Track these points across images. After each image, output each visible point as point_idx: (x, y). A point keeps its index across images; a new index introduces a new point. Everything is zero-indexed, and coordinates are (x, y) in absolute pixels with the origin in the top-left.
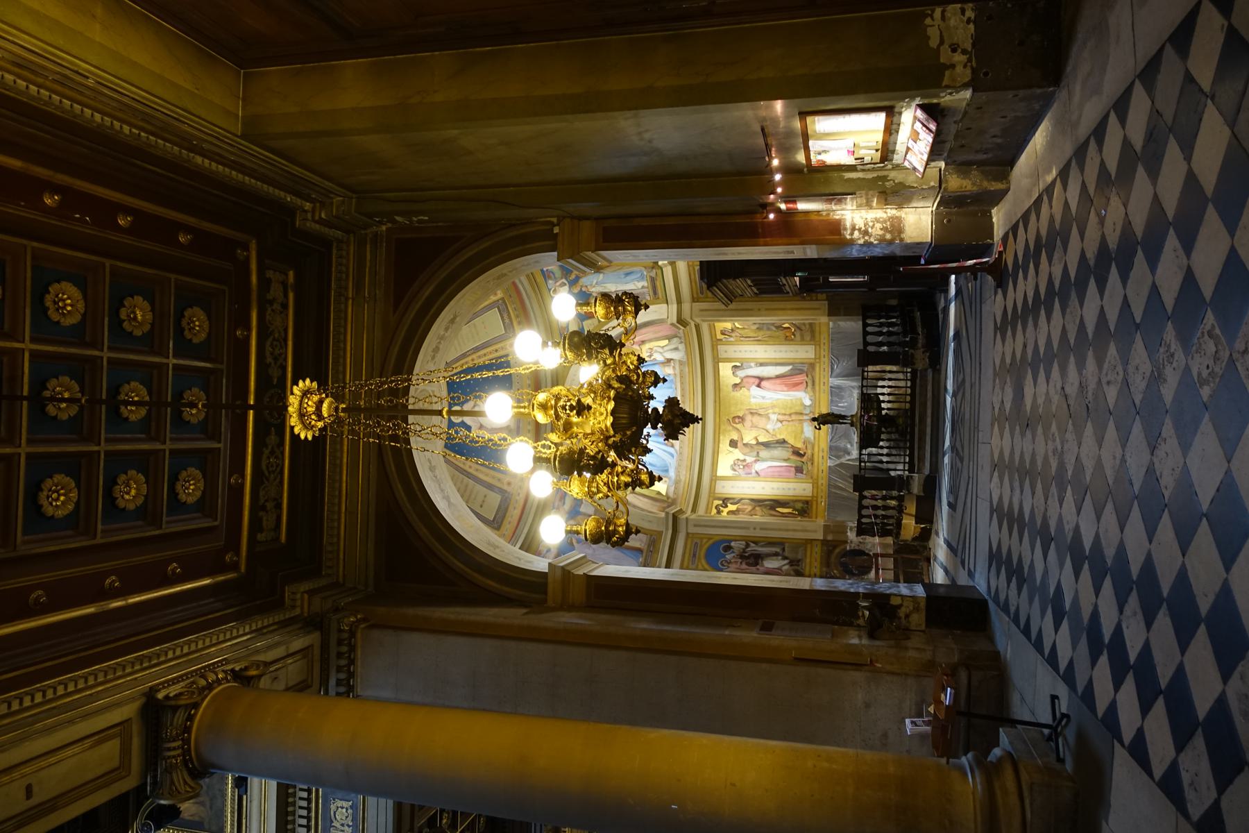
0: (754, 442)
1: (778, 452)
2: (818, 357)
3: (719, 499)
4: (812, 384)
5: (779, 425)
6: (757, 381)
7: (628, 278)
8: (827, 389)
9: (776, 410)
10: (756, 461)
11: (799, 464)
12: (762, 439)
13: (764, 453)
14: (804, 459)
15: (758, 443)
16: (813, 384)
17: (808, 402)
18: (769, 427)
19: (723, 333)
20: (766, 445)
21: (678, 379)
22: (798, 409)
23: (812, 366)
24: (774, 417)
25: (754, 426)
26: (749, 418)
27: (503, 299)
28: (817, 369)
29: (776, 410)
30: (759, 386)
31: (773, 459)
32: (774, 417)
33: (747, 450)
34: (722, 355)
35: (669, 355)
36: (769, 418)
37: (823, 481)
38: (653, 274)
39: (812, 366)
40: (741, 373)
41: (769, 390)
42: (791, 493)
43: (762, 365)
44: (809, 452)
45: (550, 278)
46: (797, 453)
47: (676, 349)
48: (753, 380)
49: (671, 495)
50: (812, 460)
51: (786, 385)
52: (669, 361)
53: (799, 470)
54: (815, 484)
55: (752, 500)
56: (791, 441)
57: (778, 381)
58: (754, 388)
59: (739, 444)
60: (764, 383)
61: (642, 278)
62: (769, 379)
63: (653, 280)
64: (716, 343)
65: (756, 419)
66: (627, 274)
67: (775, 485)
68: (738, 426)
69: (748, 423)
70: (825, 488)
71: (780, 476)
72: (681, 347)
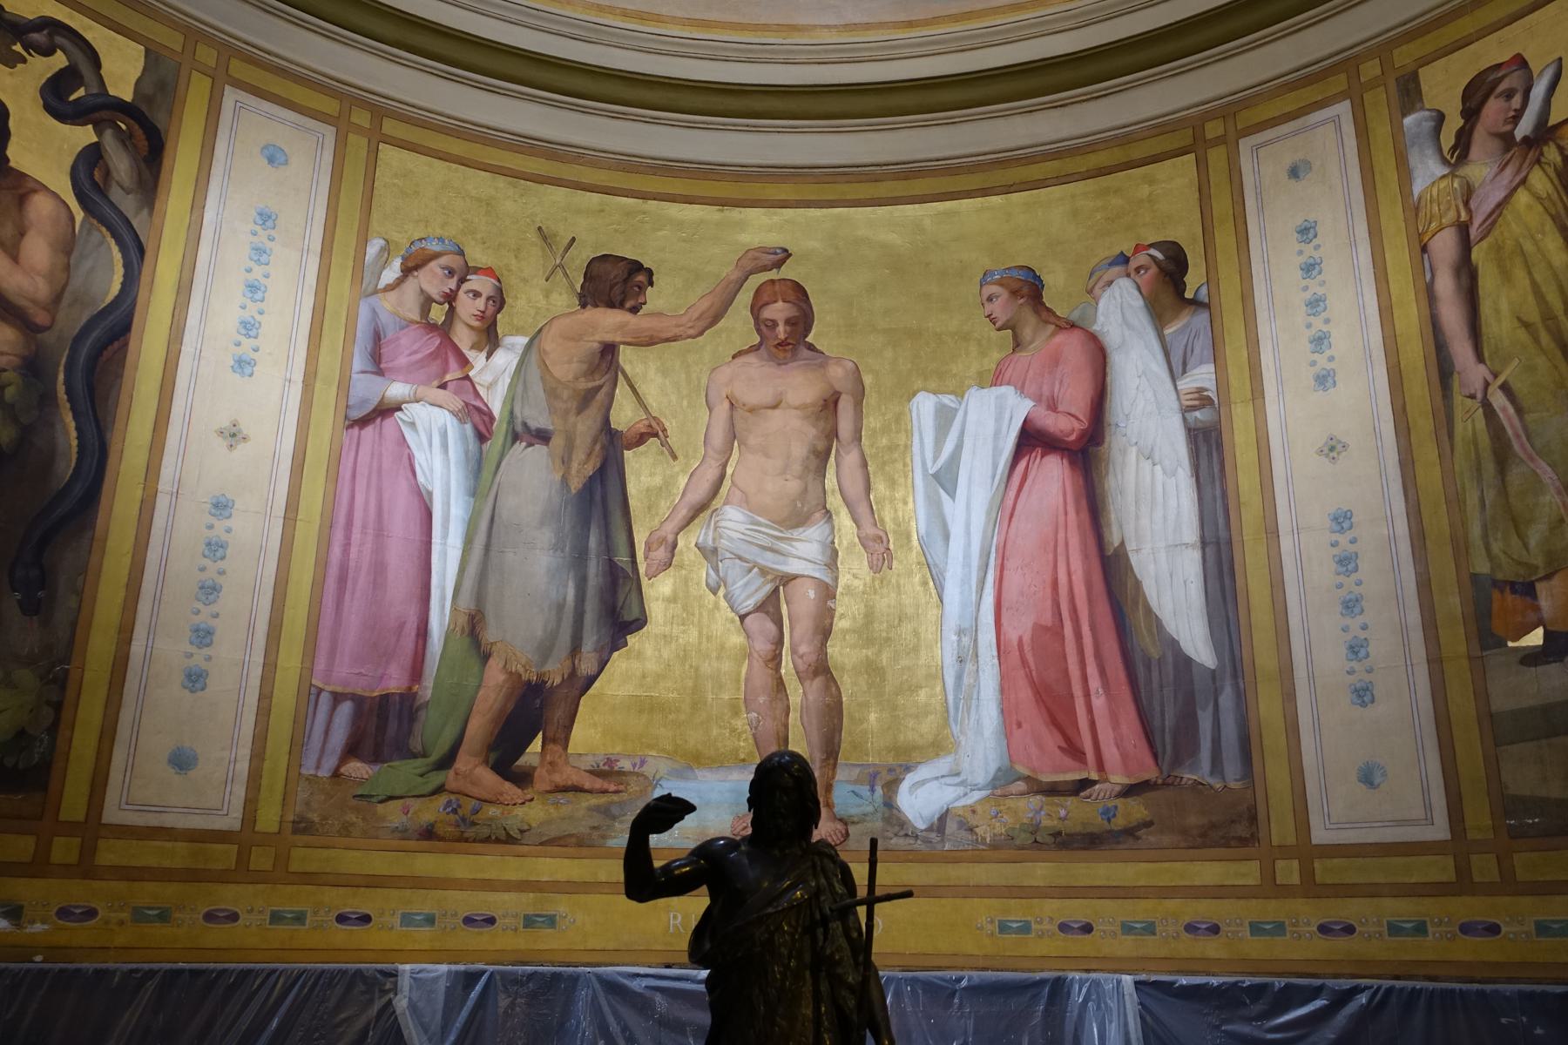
0: (624, 415)
1: (538, 574)
2: (1319, 872)
3: (162, 81)
4: (1061, 821)
5: (750, 592)
6: (1065, 425)
8: (1040, 949)
9: (854, 571)
10: (479, 421)
11: (434, 731)
12: (642, 472)
13: (533, 479)
14: (474, 771)
15: (612, 448)
16: (1067, 842)
17: (921, 799)
18: (733, 520)
19: (1475, 96)
20: (599, 499)
22: (868, 723)
23: (1234, 826)
24: (802, 553)
25: (738, 421)
26: (800, 386)
28: (1208, 872)
29: (854, 571)
30: (1031, 440)
31: (488, 537)
32: (802, 553)
33: (567, 365)
34: (1262, 162)
36: (796, 519)
37: (255, 928)
39: (1234, 826)
40: (1120, 312)
41: (1006, 511)
42: (161, 646)
43: (1207, 443)
44: (533, 812)
46: (534, 712)
48: (1076, 397)
50: (467, 831)
51: (1049, 634)
53: (382, 726)
54: (236, 855)
55: (113, 330)
56: (628, 673)
57: (1077, 567)
58: (1016, 407)
59: (608, 322)
60: (1052, 474)
62: (1093, 505)
65: (790, 432)
67: (255, 530)
68: (739, 325)
69: (757, 380)
70: (187, 936)
71: (335, 580)
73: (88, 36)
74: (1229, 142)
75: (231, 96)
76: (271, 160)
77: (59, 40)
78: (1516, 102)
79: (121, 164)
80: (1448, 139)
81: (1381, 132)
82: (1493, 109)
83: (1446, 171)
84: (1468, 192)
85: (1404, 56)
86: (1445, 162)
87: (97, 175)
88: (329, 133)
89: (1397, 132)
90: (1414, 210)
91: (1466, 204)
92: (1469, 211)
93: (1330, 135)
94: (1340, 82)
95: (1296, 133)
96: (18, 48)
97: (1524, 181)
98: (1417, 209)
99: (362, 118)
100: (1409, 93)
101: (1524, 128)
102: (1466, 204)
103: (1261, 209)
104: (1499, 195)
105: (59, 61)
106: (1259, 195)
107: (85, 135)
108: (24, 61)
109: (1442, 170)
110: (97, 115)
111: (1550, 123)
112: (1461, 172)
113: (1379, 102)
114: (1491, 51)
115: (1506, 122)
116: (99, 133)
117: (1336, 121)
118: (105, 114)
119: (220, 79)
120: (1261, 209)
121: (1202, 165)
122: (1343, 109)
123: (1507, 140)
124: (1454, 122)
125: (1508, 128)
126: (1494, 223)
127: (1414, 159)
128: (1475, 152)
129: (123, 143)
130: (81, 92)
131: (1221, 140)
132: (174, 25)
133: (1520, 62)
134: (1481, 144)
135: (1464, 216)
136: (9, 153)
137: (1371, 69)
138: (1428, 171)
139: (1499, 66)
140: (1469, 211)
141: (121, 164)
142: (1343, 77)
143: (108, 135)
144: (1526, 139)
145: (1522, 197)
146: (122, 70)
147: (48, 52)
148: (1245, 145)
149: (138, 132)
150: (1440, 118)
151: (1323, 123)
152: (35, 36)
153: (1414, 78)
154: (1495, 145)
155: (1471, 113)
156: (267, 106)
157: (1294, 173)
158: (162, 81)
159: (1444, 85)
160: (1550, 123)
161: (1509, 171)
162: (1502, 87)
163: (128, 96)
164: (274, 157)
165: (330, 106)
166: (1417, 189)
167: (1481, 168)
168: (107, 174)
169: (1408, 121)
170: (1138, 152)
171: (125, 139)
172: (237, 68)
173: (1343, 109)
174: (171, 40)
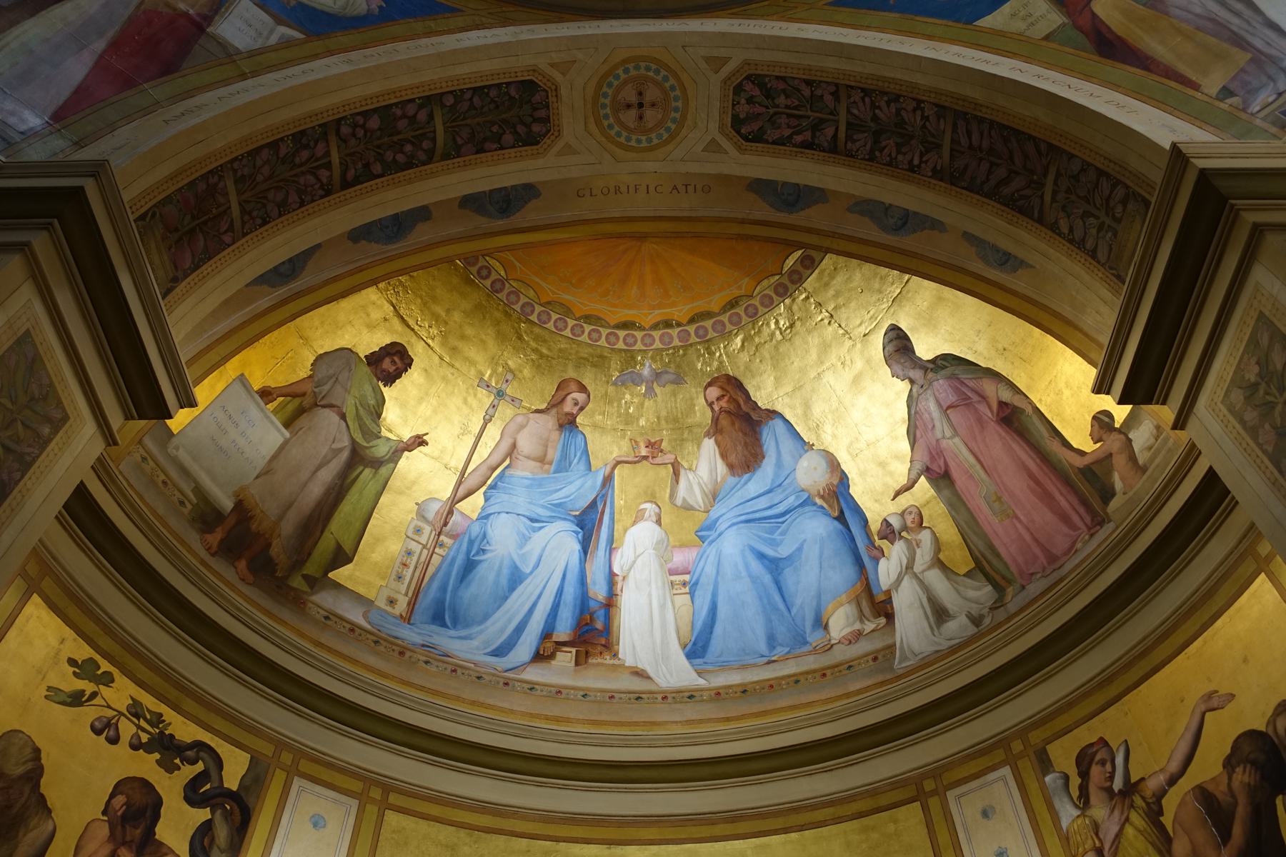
3: (256, 778)
19: (1084, 761)
21: (811, 663)
34: (964, 806)
35: (907, 603)
47: (940, 614)
49: (324, 599)
52: (882, 608)
64: (1024, 753)
72: (957, 627)
73: (219, 751)
74: (940, 792)
75: (297, 783)
76: (315, 825)
77: (202, 754)
78: (1108, 767)
79: (222, 833)
80: (1075, 793)
81: (1033, 786)
82: (1095, 770)
83: (1079, 813)
84: (1096, 827)
85: (1036, 737)
86: (1077, 807)
87: (206, 841)
88: (354, 803)
89: (1043, 787)
90: (1065, 839)
91: (1097, 834)
92: (1100, 840)
93: (1000, 787)
94: (1000, 755)
95: (981, 787)
96: (177, 761)
97: (1127, 820)
98: (1068, 839)
99: (376, 793)
100: (1044, 763)
101: (1118, 784)
102: (1097, 834)
103: (969, 840)
104: (1115, 829)
105: (200, 766)
106: (966, 830)
107: (204, 814)
108: (179, 769)
109: (1076, 813)
110: (214, 802)
111: (1133, 781)
112: (1088, 813)
113: (1027, 766)
114: (1085, 736)
115: (1106, 780)
116: (213, 813)
117: (1003, 779)
118: (219, 800)
119: (293, 772)
120: (969, 840)
121: (926, 809)
122: (1006, 771)
123: (1109, 790)
124: (1075, 781)
125: (1108, 784)
126: (1117, 848)
127: (1057, 804)
128: (1093, 799)
129: (226, 819)
130: (208, 786)
131: (934, 793)
132: (270, 739)
133: (1103, 742)
134: (1095, 796)
135: (1098, 844)
136: (157, 829)
137: (1017, 746)
138: (1068, 813)
139: (1092, 745)
140: (1100, 840)
141: (222, 833)
142: (1001, 751)
143: (219, 812)
144: (1120, 791)
145: (1129, 830)
146: (235, 770)
147: (193, 762)
148: (951, 795)
149: (237, 810)
150: (1066, 778)
151: (995, 781)
152: (189, 753)
153: (1044, 751)
154: (1104, 795)
155: (1084, 774)
156: (318, 788)
157: (985, 814)
158: (256, 778)
159: (1064, 754)
160: (1133, 781)
161: (1117, 813)
162: (1098, 757)
163: (235, 788)
164: (317, 822)
165: (357, 786)
166: (1064, 824)
167: (1099, 811)
168: (212, 840)
169: (1047, 779)
170: (884, 800)
171: (227, 816)
172: (305, 766)
173: (1006, 771)
174: (267, 749)
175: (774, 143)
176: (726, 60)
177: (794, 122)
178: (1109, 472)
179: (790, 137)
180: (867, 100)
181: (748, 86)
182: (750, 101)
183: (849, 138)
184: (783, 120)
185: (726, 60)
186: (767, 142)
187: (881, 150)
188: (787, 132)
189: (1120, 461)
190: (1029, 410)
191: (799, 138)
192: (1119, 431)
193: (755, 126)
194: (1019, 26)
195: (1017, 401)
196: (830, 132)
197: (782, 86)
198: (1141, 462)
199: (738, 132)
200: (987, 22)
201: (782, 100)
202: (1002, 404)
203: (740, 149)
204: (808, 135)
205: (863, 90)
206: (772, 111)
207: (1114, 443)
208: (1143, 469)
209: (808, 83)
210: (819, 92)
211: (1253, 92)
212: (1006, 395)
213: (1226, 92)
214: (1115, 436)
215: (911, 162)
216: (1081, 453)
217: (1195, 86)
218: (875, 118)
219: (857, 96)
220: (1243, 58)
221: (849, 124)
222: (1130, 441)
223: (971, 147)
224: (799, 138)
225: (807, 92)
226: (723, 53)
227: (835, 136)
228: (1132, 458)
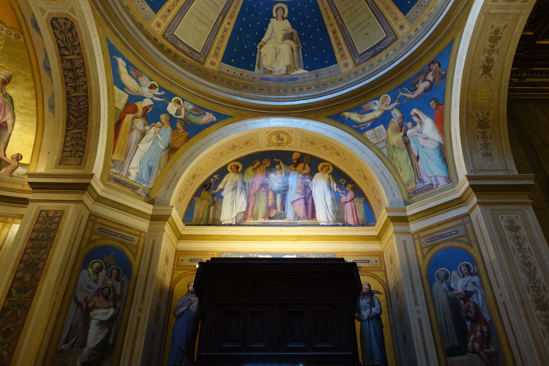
7: (145, 168)
27: (203, 64)
38: (140, 191)
45: (195, 110)
61: (139, 178)
63: (134, 188)
66: (150, 169)
175: (55, 33)
176: (75, 14)
177: (65, 40)
178: (4, 167)
179: (59, 39)
180: (81, 65)
181: (69, 23)
182: (65, 23)
183: (67, 60)
184: (64, 36)
185: (75, 14)
186: (54, 31)
187: (67, 72)
188: (60, 37)
189: (10, 168)
190: (9, 132)
191: (60, 42)
192: (18, 163)
193: (57, 26)
194: (117, 98)
195: (10, 127)
196: (67, 53)
197: (74, 34)
198: (13, 174)
199: (52, 20)
200: (116, 88)
201: (70, 35)
202: (5, 123)
203: (47, 21)
204: (62, 45)
205: (83, 63)
206: (65, 31)
207: (14, 163)
208: (11, 176)
209: (79, 44)
210: (77, 48)
211: (115, 167)
212: (9, 122)
213: (113, 161)
214: (16, 163)
215: (68, 83)
216: (5, 155)
217: (113, 153)
218: (77, 69)
219: (81, 61)
220: (122, 159)
221: (72, 59)
222: (17, 167)
223: (79, 102)
224: (60, 42)
225: (76, 44)
226: (77, 13)
227: (66, 55)
228: (13, 171)
